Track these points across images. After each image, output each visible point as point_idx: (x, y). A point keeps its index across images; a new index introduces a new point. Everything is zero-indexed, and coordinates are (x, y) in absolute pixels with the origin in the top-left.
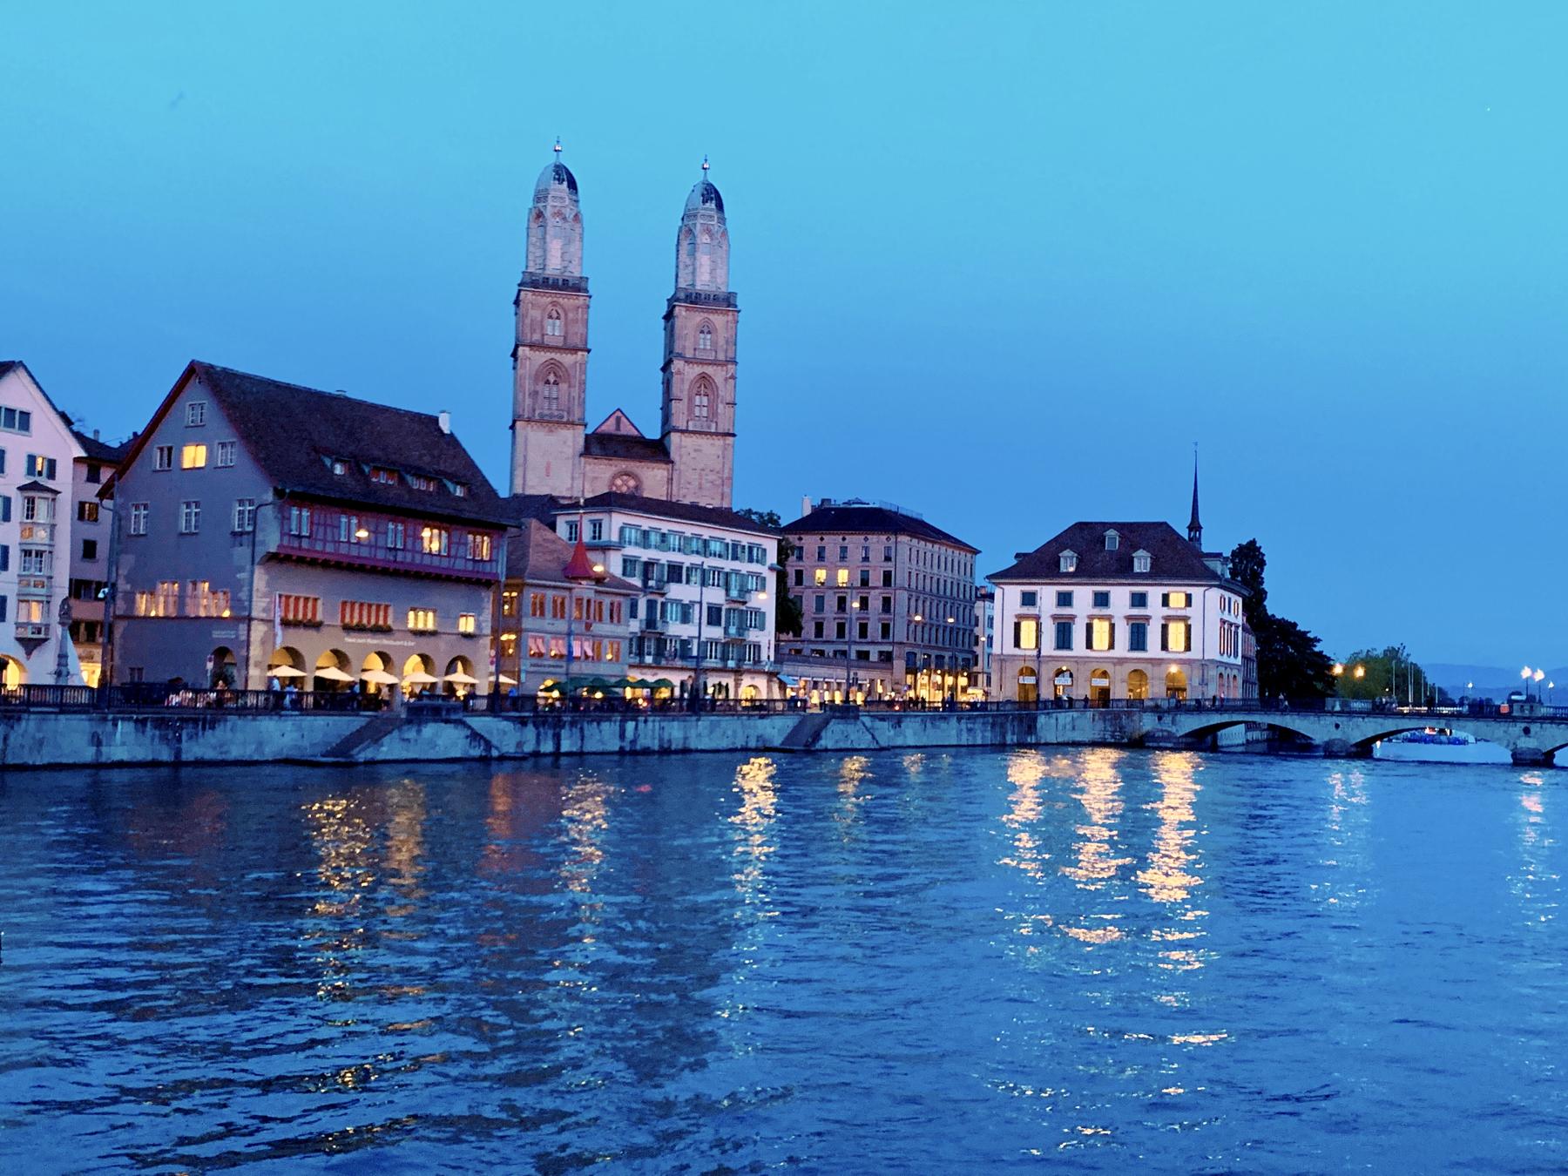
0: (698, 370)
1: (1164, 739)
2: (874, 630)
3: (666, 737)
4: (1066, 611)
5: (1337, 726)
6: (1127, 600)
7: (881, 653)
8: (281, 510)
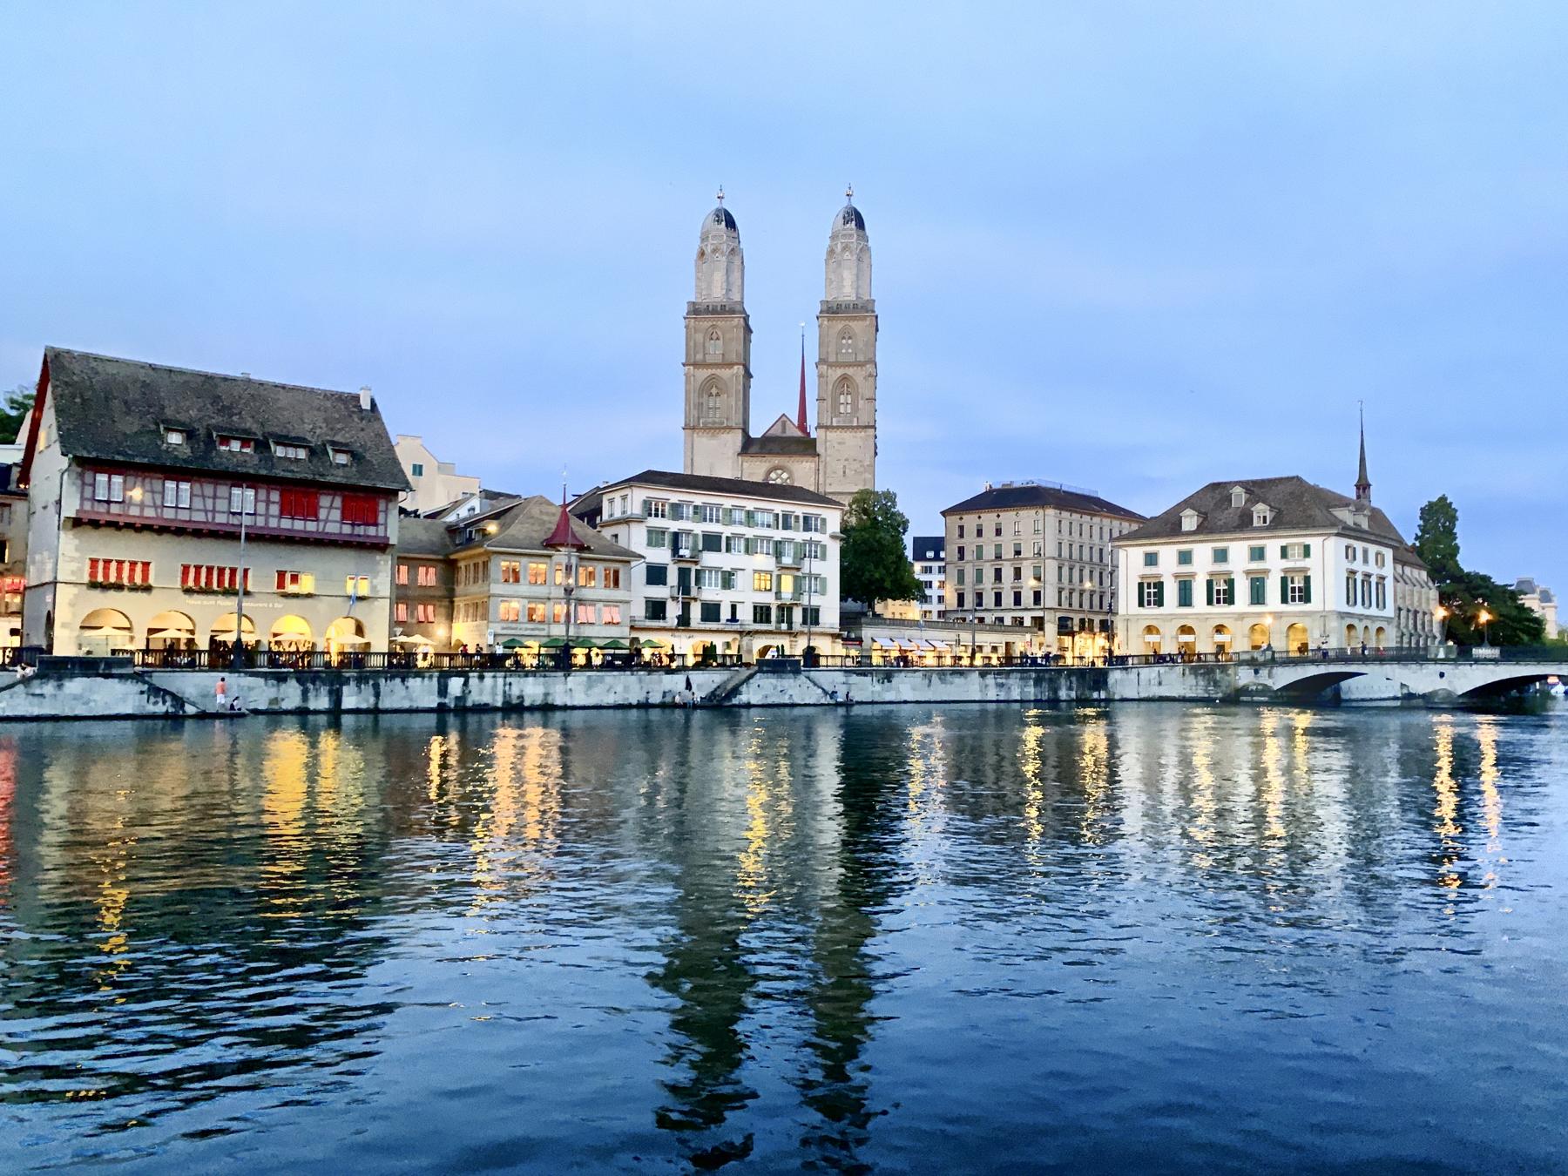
0: (840, 372)
1: (1258, 693)
2: (1027, 598)
3: (515, 691)
4: (1185, 569)
5: (1442, 675)
6: (1246, 554)
7: (1014, 618)
8: (81, 476)
